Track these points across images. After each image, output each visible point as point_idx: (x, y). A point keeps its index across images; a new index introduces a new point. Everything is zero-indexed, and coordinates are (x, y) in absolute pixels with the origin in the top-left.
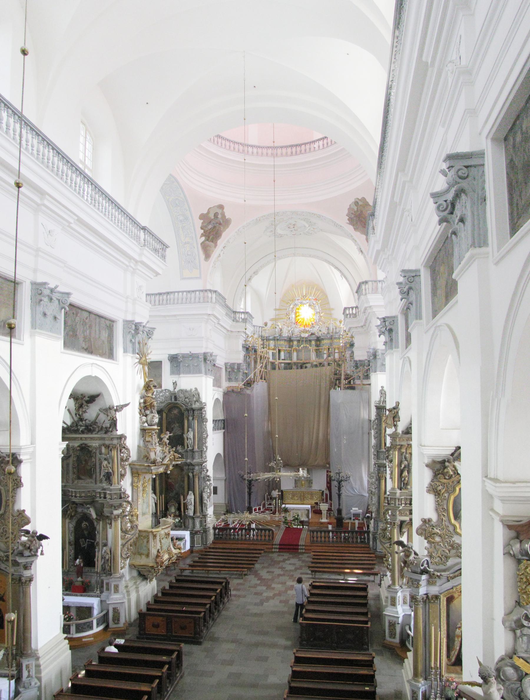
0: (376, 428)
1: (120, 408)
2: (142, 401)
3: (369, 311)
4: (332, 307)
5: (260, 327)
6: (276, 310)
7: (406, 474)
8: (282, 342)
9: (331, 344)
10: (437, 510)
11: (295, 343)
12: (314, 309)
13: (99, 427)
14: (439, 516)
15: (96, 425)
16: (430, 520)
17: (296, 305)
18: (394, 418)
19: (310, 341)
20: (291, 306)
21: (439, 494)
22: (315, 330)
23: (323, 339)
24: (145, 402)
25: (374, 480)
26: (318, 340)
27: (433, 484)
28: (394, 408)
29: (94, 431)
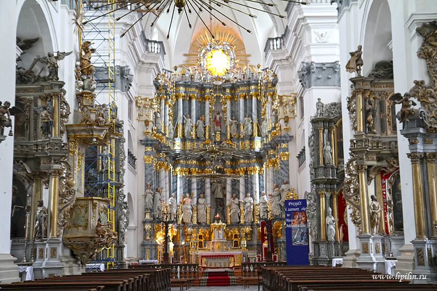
0: (312, 146)
1: (61, 56)
2: (78, 63)
3: (302, 23)
4: (247, 53)
5: (168, 71)
6: (185, 55)
7: (371, 117)
8: (193, 89)
9: (249, 91)
10: (428, 72)
11: (208, 91)
12: (228, 55)
13: (35, 76)
14: (430, 76)
15: (31, 75)
16: (422, 82)
17: (207, 50)
18: (357, 61)
19: (224, 89)
20: (204, 51)
21: (430, 56)
22: (231, 76)
23: (238, 87)
24: (81, 66)
25: (312, 201)
26: (234, 88)
27: (423, 48)
28: (356, 52)
29: (29, 81)
